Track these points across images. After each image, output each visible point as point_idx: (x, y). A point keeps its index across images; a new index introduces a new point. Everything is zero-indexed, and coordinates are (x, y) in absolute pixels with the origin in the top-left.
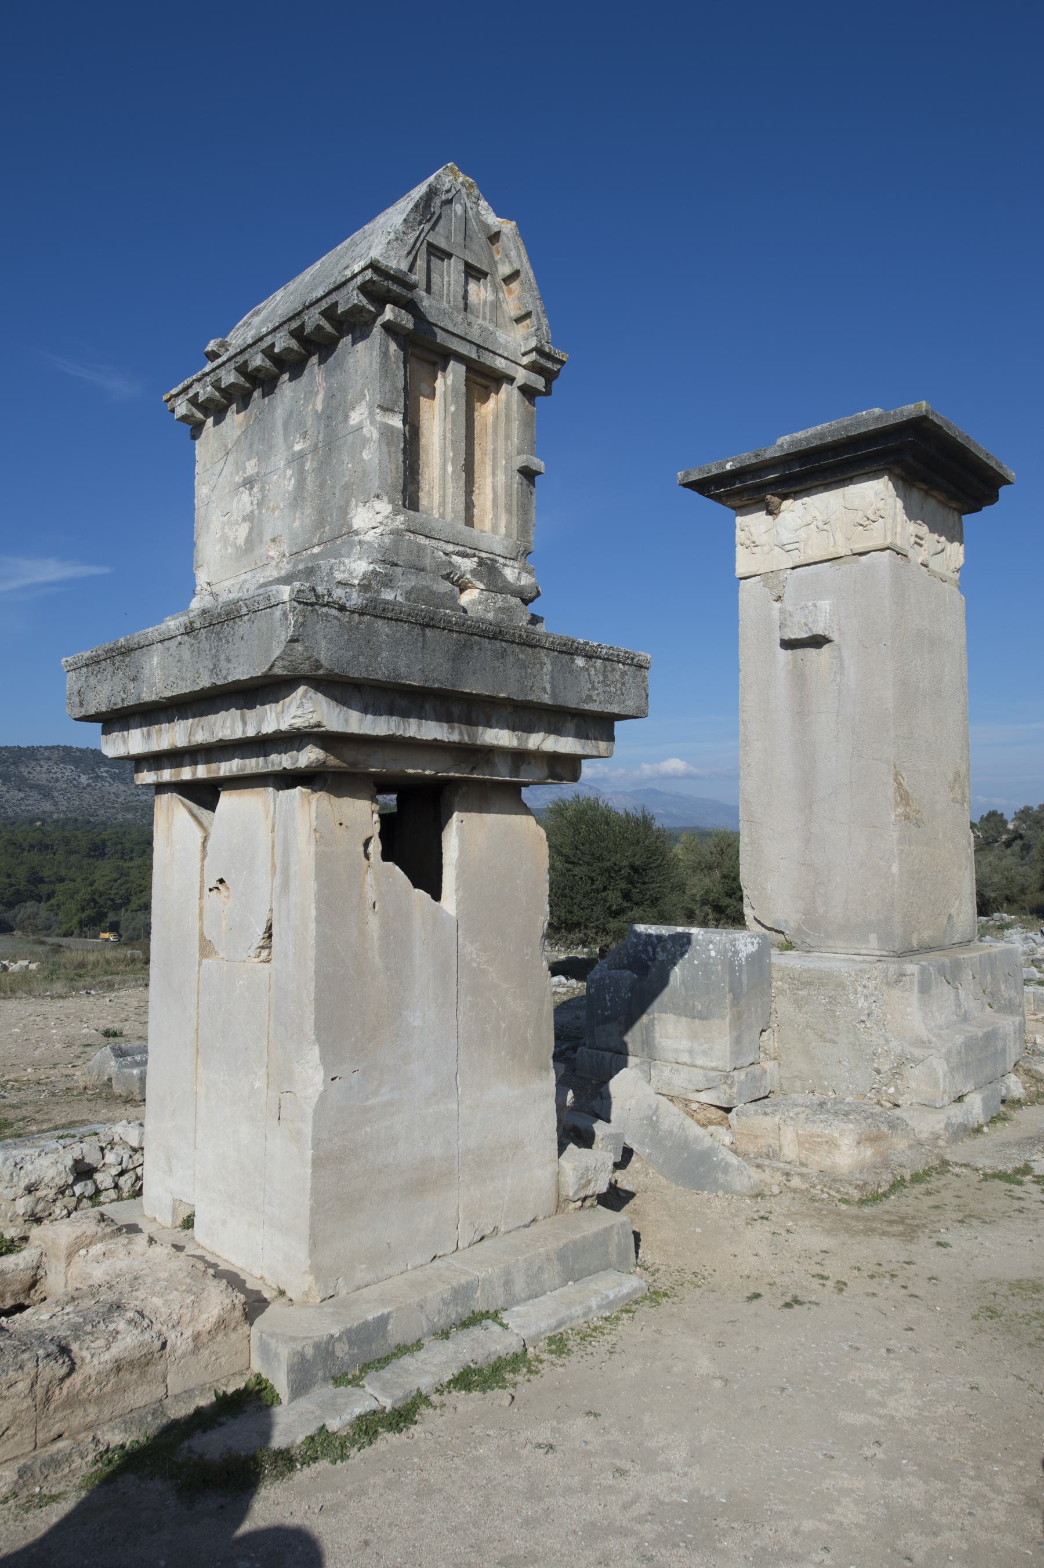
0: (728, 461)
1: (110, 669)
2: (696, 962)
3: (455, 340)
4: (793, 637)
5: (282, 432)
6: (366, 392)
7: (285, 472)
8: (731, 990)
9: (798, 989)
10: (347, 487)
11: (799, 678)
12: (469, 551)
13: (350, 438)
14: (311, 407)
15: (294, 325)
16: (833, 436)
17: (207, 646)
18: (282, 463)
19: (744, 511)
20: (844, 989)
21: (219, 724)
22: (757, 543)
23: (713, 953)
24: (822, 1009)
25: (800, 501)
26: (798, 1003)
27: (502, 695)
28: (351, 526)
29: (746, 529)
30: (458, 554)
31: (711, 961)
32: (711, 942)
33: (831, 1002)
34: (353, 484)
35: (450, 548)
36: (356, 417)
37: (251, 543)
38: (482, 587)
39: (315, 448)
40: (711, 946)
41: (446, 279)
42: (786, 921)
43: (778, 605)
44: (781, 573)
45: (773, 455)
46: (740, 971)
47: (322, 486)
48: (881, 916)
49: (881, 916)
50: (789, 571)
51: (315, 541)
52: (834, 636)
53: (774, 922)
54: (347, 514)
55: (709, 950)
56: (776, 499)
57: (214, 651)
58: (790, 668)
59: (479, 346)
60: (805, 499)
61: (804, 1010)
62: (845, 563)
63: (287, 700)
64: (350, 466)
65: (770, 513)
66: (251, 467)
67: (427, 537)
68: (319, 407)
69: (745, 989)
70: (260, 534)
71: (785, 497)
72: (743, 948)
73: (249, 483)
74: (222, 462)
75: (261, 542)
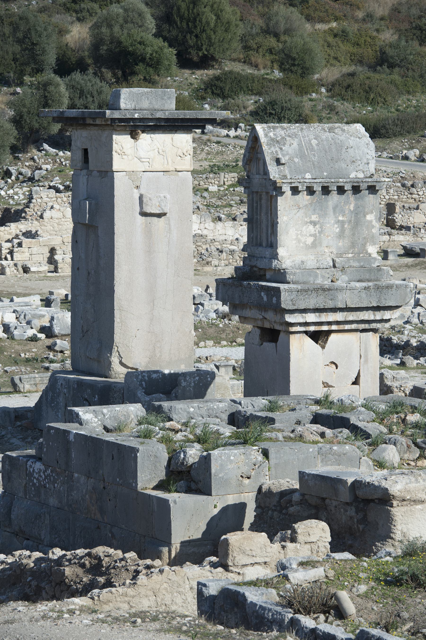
0: (136, 113)
1: (316, 295)
4: (152, 212)
5: (332, 210)
7: (334, 225)
10: (365, 238)
11: (148, 233)
14: (347, 207)
16: (190, 116)
17: (375, 294)
18: (333, 222)
19: (117, 132)
20: (228, 389)
21: (361, 315)
22: (126, 153)
25: (149, 135)
29: (119, 144)
36: (369, 217)
37: (314, 245)
39: (350, 221)
40: (208, 376)
42: (140, 363)
45: (160, 117)
47: (353, 234)
48: (187, 356)
49: (187, 356)
50: (142, 173)
51: (351, 252)
56: (140, 132)
58: (144, 227)
60: (152, 135)
63: (395, 311)
65: (132, 137)
66: (314, 218)
68: (352, 209)
70: (321, 244)
71: (143, 132)
73: (314, 224)
75: (321, 246)
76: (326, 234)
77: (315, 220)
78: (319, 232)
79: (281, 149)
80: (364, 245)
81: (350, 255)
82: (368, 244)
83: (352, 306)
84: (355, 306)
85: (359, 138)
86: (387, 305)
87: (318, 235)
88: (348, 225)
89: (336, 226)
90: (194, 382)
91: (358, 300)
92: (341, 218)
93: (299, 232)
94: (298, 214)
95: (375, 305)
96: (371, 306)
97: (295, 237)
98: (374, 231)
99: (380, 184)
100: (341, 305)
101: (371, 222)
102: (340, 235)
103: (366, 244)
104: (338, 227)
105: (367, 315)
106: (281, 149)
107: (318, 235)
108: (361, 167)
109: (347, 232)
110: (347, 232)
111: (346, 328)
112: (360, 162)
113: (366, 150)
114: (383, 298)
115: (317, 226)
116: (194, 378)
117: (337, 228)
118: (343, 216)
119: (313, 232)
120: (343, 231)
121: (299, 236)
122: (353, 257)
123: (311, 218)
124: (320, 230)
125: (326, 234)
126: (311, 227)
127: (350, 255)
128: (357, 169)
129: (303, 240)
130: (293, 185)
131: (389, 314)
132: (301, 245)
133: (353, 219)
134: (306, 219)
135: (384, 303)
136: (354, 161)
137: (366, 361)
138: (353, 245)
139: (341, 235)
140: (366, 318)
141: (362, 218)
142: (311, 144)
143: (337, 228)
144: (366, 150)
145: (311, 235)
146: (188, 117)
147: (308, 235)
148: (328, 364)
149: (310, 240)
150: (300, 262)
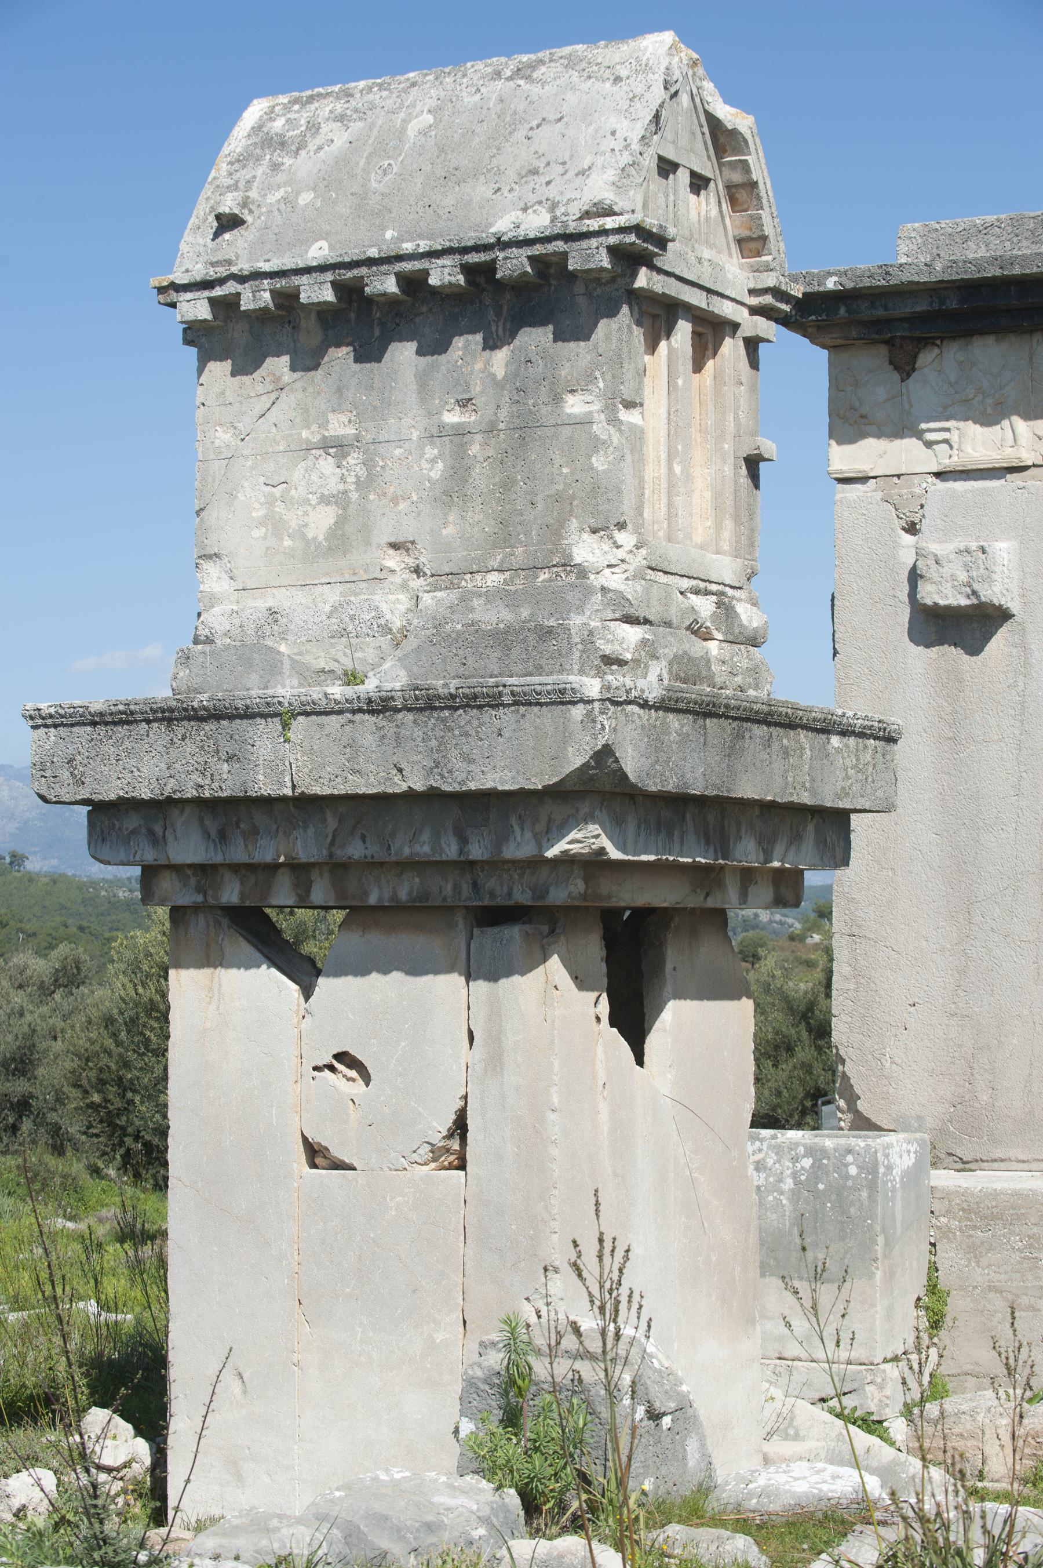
2: (821, 1186)
3: (687, 288)
4: (942, 602)
5: (414, 387)
6: (597, 374)
7: (421, 447)
8: (883, 1231)
9: (975, 1228)
10: (558, 498)
12: (702, 585)
13: (566, 432)
14: (479, 366)
15: (474, 258)
17: (418, 733)
18: (415, 435)
23: (853, 1170)
24: (1016, 1256)
26: (974, 1251)
27: (769, 798)
28: (570, 556)
30: (697, 592)
31: (850, 1183)
32: (849, 1151)
33: (1031, 1246)
34: (573, 497)
35: (685, 584)
37: (338, 541)
38: (720, 637)
39: (491, 430)
41: (671, 198)
43: (908, 539)
44: (916, 479)
46: (893, 1199)
47: (507, 485)
50: (931, 479)
51: (494, 563)
52: (1014, 606)
53: (896, 1120)
54: (560, 537)
55: (846, 1165)
57: (434, 743)
59: (709, 291)
61: (984, 1261)
62: (1033, 478)
64: (565, 470)
66: (340, 426)
67: (666, 573)
69: (899, 1231)
70: (366, 532)
72: (898, 1161)
73: (337, 448)
74: (266, 401)
75: (368, 543)
76: (391, 490)
77: (341, 431)
78: (358, 482)
79: (276, 167)
80: (555, 531)
81: (494, 579)
82: (574, 524)
83: (317, 790)
84: (327, 791)
85: (618, 79)
86: (472, 786)
87: (354, 496)
88: (485, 444)
89: (431, 452)
90: (795, 1176)
91: (342, 760)
92: (452, 417)
93: (277, 491)
94: (273, 415)
95: (419, 786)
96: (404, 787)
97: (259, 513)
98: (599, 462)
99: (584, 244)
100: (264, 786)
101: (586, 422)
102: (447, 493)
103: (562, 522)
104: (440, 455)
105: (426, 836)
106: (276, 167)
107: (354, 496)
108: (552, 192)
109: (481, 476)
110: (481, 476)
111: (372, 900)
112: (560, 169)
113: (614, 121)
114: (454, 753)
115: (353, 459)
116: (795, 1160)
117: (433, 461)
118: (464, 403)
119: (334, 486)
120: (459, 471)
121: (279, 508)
122: (505, 582)
123: (324, 425)
124: (362, 472)
125: (391, 490)
126: (327, 465)
127: (494, 579)
128: (532, 198)
129: (294, 524)
130: (218, 292)
131: (528, 835)
132: (287, 543)
133: (503, 414)
134: (305, 434)
135: (460, 776)
136: (535, 172)
137: (495, 1062)
138: (504, 534)
139: (453, 490)
140: (424, 849)
141: (544, 410)
142: (403, 130)
143: (433, 461)
144: (614, 121)
145: (324, 500)
146: (1017, 270)
147: (314, 499)
148: (328, 1059)
149: (322, 521)
150: (267, 614)
